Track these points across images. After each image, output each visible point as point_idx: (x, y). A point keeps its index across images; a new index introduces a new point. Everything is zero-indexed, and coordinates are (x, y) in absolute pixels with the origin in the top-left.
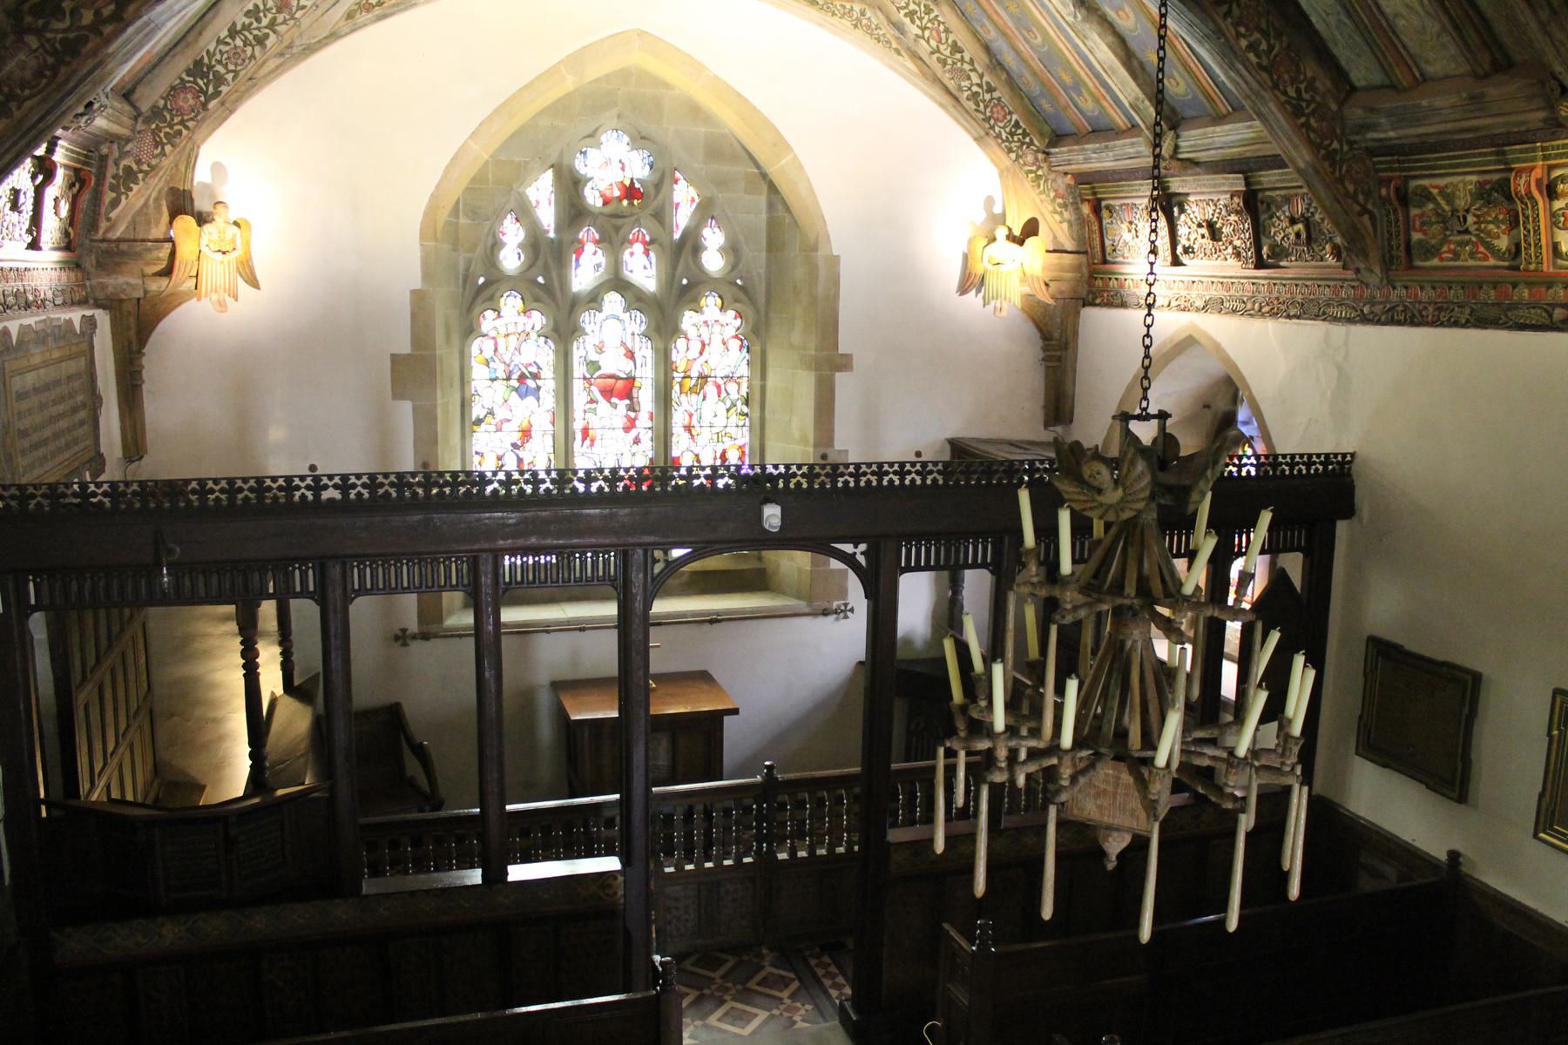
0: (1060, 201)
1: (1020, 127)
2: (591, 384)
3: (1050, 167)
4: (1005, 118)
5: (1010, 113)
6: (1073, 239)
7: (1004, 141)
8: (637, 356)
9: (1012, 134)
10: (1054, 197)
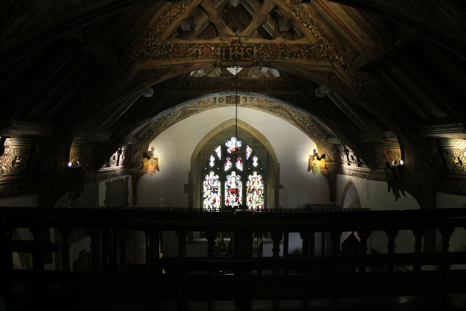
0: (331, 150)
1: (320, 134)
2: (229, 191)
3: (327, 142)
4: (316, 132)
5: (317, 131)
6: (334, 158)
7: (316, 137)
9: (318, 136)
10: (329, 149)
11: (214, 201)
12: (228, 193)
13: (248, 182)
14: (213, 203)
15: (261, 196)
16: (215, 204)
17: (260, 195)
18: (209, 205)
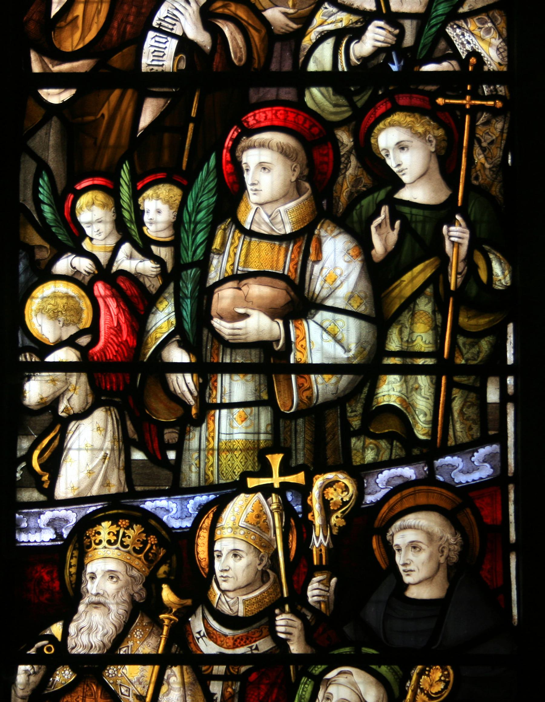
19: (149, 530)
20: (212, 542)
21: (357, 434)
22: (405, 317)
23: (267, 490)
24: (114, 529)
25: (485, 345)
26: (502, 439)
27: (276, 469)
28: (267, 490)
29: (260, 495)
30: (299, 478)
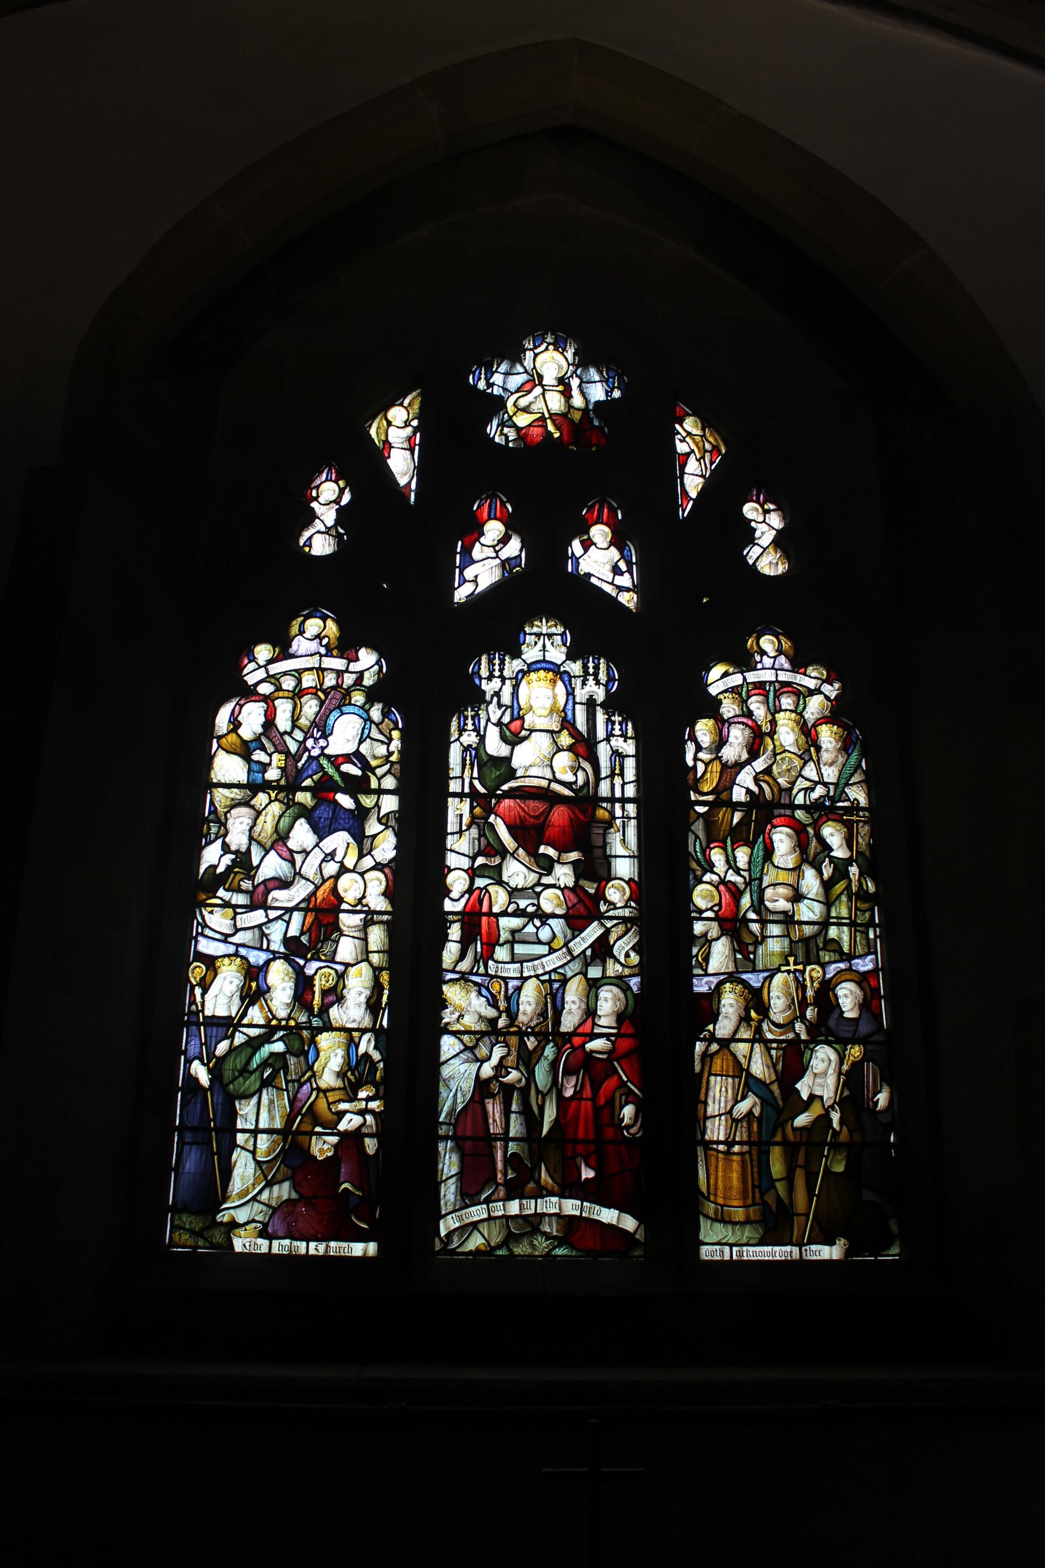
2: (489, 811)
8: (603, 752)
11: (317, 923)
12: (485, 829)
13: (704, 729)
14: (304, 939)
15: (846, 875)
16: (327, 948)
17: (841, 869)
18: (257, 958)
19: (745, 987)
20: (769, 993)
21: (822, 949)
22: (837, 903)
23: (789, 972)
24: (731, 986)
25: (867, 915)
26: (876, 953)
27: (792, 963)
28: (789, 972)
29: (786, 973)
30: (800, 967)
